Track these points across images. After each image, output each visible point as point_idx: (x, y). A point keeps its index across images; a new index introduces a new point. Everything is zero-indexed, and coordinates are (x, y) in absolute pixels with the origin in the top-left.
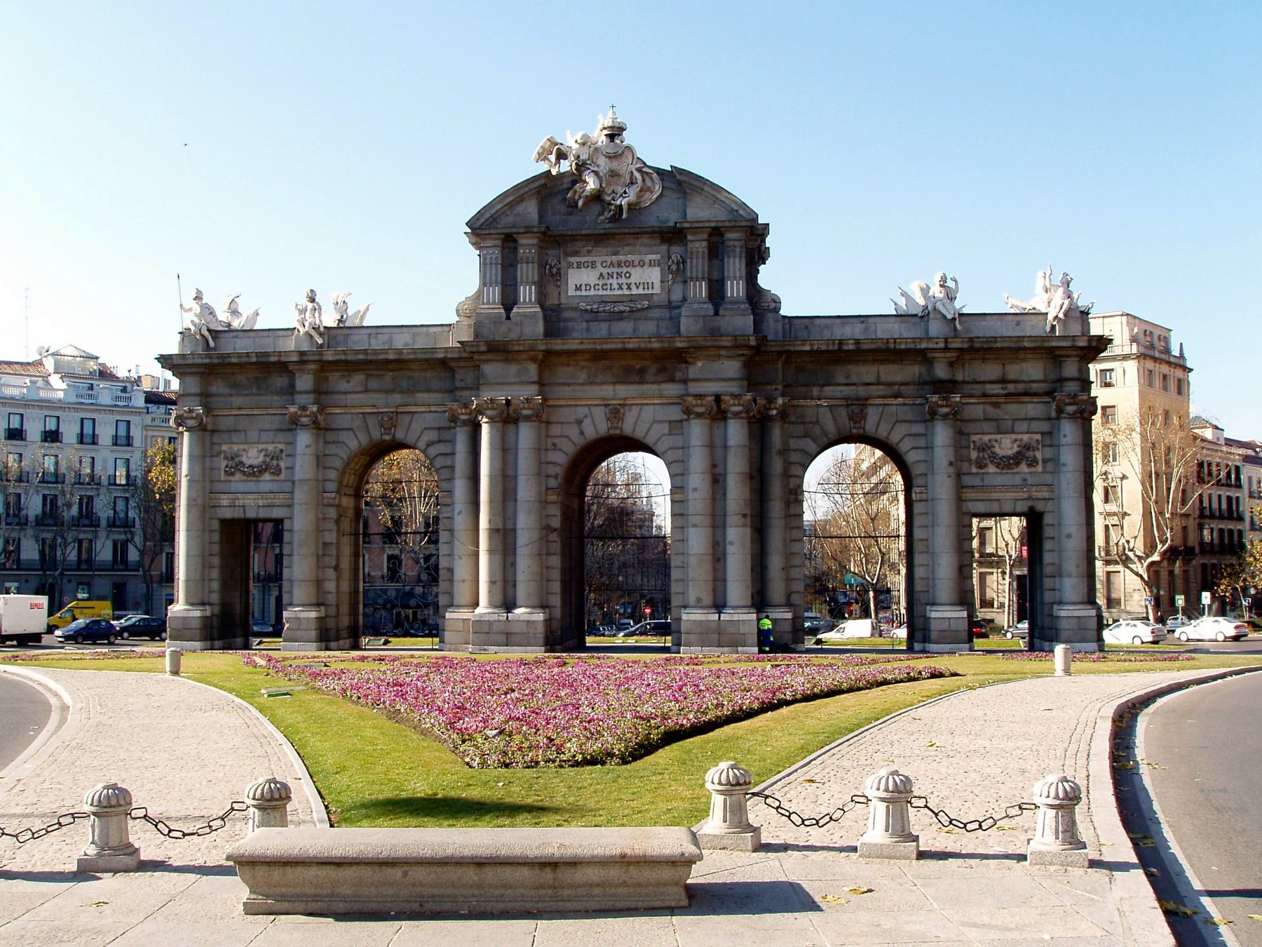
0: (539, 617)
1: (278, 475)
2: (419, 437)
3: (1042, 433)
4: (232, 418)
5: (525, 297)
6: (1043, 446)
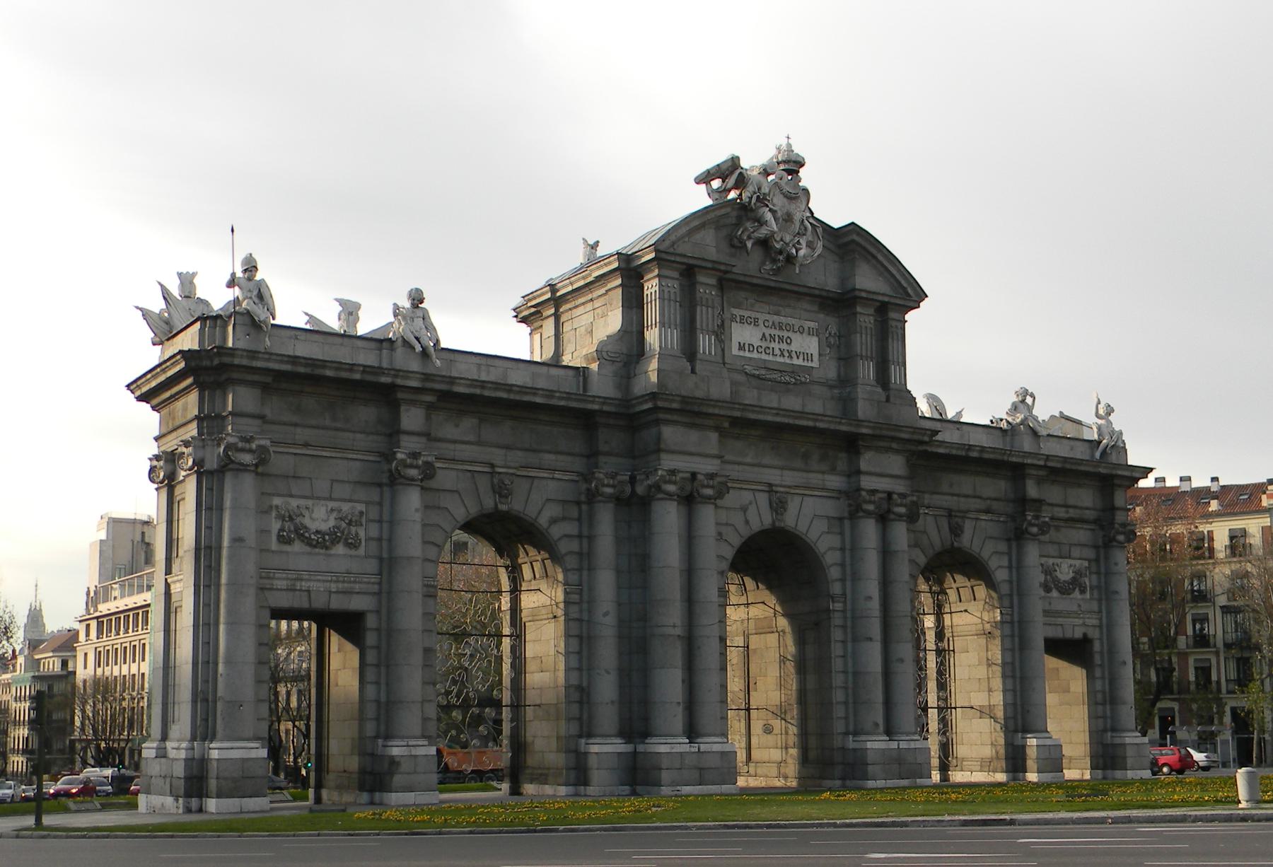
3: (1090, 561)
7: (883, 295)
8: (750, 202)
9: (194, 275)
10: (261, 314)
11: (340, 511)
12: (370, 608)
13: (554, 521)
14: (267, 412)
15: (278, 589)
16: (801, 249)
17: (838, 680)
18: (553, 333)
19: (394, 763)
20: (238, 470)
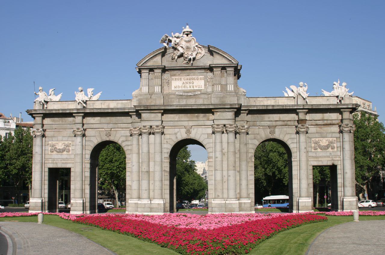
0: (163, 202)
3: (336, 138)
4: (53, 132)
5: (157, 90)
6: (337, 142)
11: (65, 143)
12: (72, 167)
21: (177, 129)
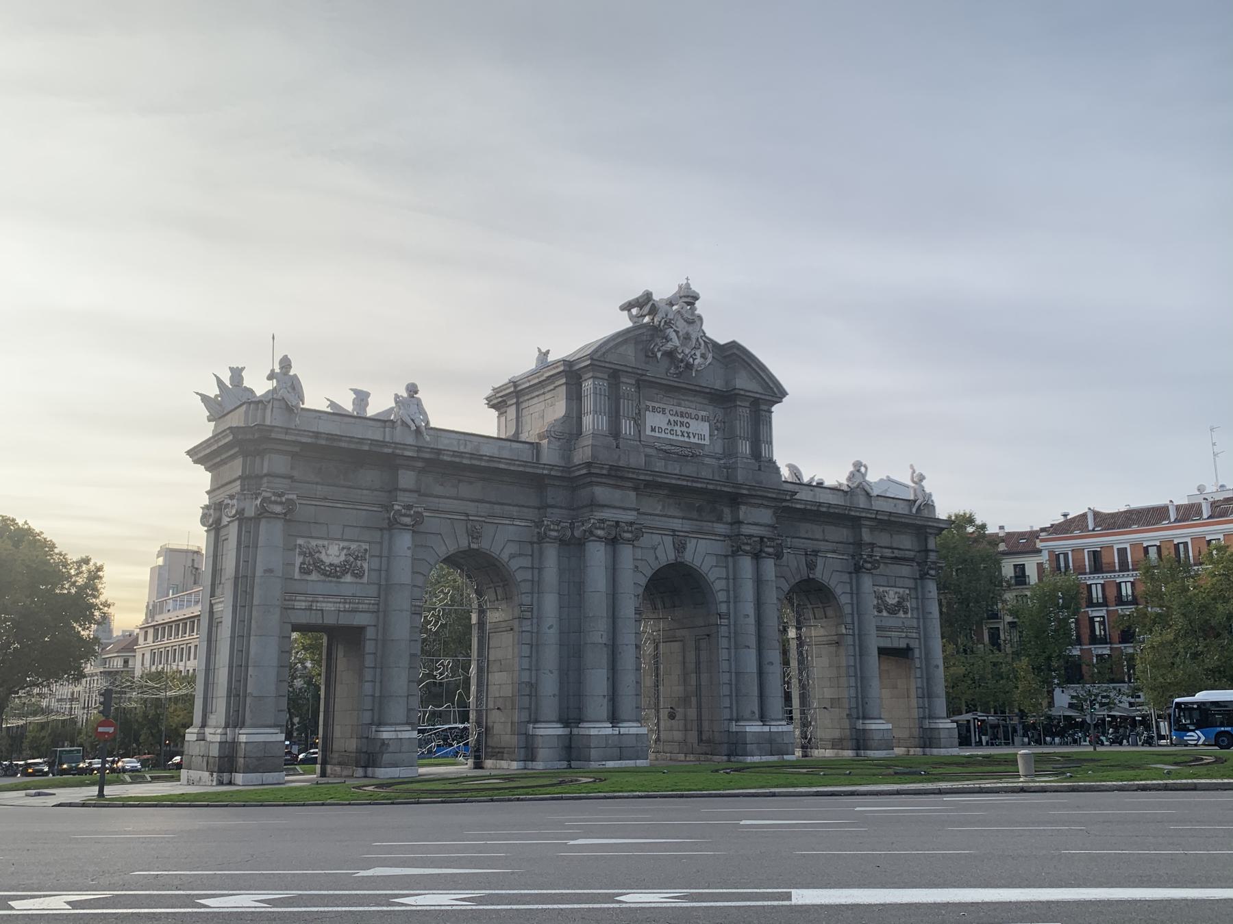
1: (361, 577)
2: (502, 550)
3: (910, 589)
5: (626, 430)
6: (911, 598)
7: (757, 393)
8: (659, 325)
9: (243, 369)
10: (292, 401)
12: (369, 624)
13: (512, 556)
14: (295, 474)
15: (297, 609)
16: (696, 359)
17: (725, 678)
18: (514, 416)
19: (384, 743)
20: (270, 517)
21: (657, 536)
